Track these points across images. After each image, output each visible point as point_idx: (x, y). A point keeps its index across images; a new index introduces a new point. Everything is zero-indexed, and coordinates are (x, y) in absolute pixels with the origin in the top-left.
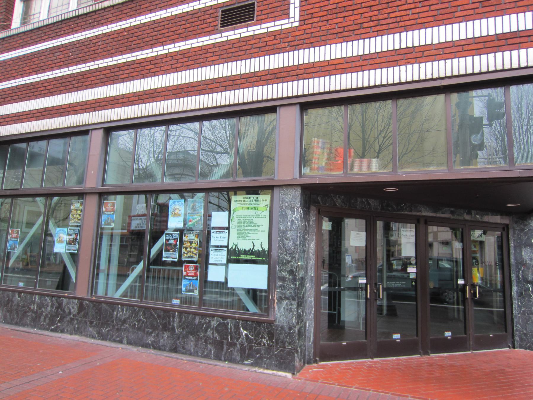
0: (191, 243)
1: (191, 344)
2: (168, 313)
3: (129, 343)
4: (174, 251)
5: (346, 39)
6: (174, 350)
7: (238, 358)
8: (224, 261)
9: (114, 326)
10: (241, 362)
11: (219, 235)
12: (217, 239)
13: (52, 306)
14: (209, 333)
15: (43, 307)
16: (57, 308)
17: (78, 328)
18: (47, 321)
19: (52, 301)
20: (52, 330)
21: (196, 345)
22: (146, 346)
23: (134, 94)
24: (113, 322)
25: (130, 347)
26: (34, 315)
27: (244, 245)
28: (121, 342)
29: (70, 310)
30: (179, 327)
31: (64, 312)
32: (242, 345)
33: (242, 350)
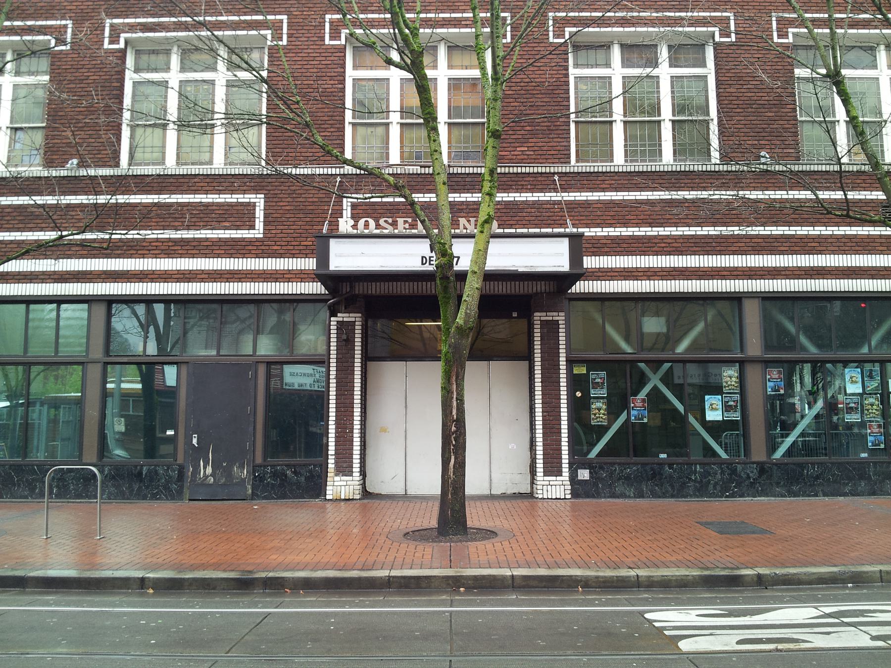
2: (863, 463)
3: (825, 495)
4: (857, 413)
9: (805, 483)
13: (723, 473)
15: (709, 474)
18: (718, 488)
19: (722, 469)
20: (727, 497)
22: (845, 495)
23: (800, 269)
24: (804, 479)
25: (827, 499)
29: (748, 475)
31: (740, 476)
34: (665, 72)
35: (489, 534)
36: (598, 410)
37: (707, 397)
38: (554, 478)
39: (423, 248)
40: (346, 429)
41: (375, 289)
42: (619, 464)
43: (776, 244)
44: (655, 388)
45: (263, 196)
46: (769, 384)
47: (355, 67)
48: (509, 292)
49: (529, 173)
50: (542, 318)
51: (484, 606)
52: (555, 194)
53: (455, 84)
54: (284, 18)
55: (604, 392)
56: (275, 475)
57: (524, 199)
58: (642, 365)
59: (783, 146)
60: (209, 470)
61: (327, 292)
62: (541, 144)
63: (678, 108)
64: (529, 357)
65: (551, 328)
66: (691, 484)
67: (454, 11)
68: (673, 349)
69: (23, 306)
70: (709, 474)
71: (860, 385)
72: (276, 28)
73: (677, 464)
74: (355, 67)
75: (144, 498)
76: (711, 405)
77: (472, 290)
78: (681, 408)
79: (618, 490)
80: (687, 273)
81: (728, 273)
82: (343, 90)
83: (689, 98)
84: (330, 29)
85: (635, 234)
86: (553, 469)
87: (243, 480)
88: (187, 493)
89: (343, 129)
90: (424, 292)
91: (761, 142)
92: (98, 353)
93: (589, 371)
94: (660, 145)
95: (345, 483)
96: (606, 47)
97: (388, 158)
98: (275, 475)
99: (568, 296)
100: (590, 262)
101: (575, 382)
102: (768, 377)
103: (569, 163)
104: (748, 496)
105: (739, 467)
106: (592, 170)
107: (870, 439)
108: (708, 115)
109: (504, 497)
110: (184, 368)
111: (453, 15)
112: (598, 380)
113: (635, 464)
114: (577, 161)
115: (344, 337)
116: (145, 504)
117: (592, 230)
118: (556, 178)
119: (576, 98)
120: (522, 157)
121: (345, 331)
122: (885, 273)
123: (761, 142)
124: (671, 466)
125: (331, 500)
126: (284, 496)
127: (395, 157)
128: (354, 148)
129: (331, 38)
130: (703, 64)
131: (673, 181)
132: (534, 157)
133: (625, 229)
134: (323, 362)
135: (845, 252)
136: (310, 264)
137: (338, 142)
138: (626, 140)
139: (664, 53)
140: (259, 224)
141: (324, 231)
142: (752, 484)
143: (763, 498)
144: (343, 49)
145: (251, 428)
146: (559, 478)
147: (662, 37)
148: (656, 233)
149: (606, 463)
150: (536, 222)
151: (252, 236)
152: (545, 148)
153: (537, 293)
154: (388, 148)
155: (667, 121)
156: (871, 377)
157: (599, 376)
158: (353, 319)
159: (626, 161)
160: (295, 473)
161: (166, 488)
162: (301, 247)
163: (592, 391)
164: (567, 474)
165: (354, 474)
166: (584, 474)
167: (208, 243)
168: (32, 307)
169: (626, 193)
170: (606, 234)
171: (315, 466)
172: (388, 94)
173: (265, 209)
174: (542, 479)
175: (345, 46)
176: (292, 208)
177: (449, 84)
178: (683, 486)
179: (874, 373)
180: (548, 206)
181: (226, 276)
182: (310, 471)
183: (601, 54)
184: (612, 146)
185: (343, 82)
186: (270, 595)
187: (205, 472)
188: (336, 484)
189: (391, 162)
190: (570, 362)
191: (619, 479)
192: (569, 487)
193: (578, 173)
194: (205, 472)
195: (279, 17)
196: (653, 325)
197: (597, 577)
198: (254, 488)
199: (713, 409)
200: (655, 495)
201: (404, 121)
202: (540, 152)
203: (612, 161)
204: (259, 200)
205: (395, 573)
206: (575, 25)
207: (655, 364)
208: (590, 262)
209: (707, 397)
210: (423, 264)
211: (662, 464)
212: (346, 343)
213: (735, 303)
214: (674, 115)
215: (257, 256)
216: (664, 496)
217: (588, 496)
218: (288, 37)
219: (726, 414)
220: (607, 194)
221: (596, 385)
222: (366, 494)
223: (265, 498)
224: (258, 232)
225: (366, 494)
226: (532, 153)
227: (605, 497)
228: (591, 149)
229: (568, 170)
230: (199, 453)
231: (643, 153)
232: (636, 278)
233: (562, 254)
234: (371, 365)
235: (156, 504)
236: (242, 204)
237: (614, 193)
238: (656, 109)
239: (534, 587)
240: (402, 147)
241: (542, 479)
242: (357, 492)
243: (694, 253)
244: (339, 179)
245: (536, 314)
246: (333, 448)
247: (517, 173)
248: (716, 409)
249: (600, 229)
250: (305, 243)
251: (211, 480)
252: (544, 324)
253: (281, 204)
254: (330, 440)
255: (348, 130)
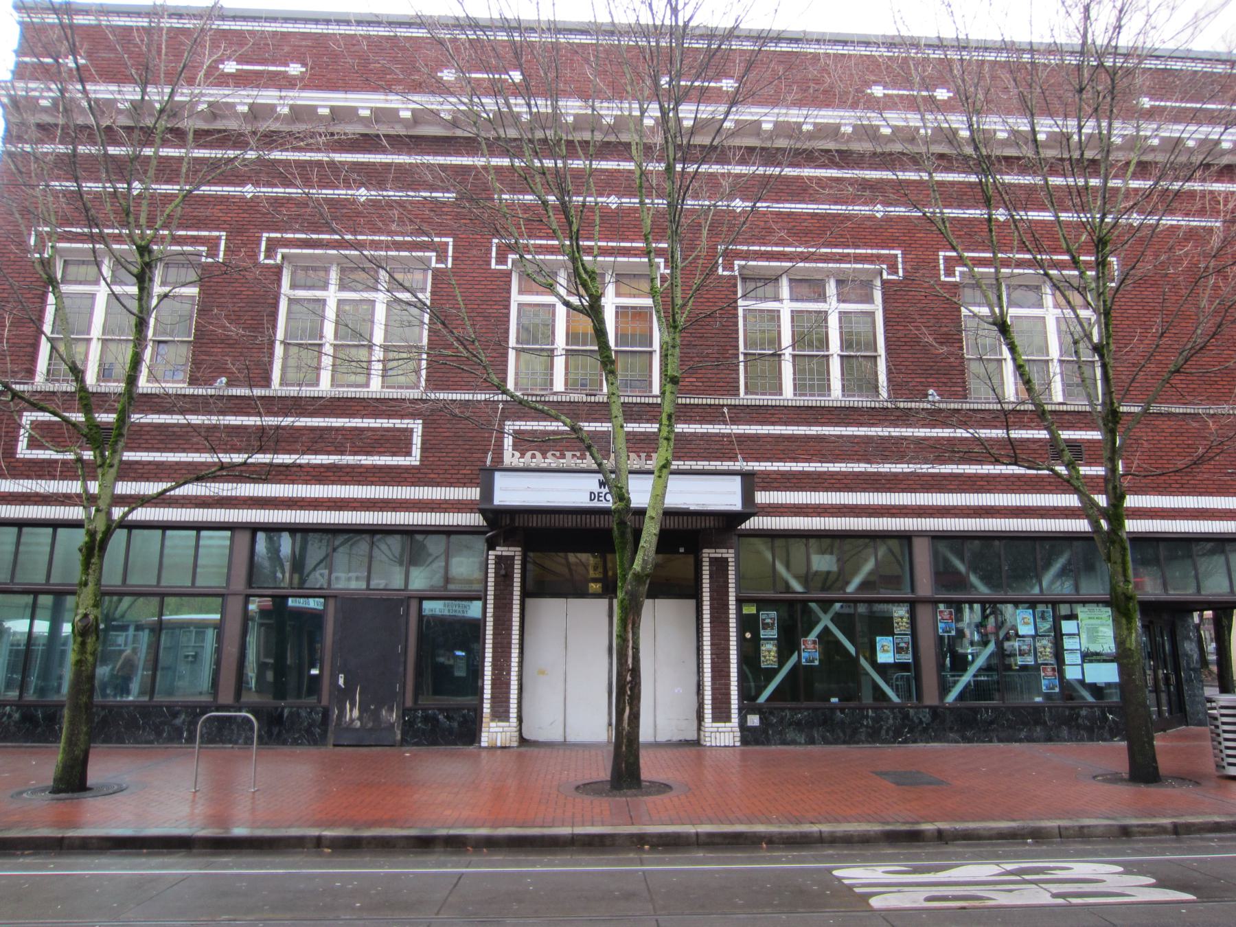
0: (1045, 648)
1: (1065, 732)
2: (1037, 709)
3: (1000, 740)
5: (1161, 493)
6: (1049, 739)
7: (1108, 737)
8: (1079, 661)
10: (1111, 739)
11: (1071, 640)
12: (1068, 643)
13: (895, 718)
14: (1080, 721)
15: (882, 720)
16: (903, 719)
17: (935, 736)
18: (891, 733)
19: (894, 713)
20: (900, 742)
21: (1070, 733)
22: (1020, 741)
25: (1002, 745)
26: (870, 730)
27: (1094, 648)
28: (990, 741)
30: (1050, 720)
31: (912, 721)
32: (1110, 727)
33: (1111, 730)
34: (833, 307)
35: (664, 788)
36: (769, 652)
37: (878, 638)
38: (723, 724)
39: (591, 483)
40: (503, 670)
41: (534, 522)
42: (790, 709)
43: (944, 482)
44: (826, 629)
45: (421, 421)
46: (940, 625)
47: (521, 292)
48: (676, 526)
49: (698, 405)
50: (712, 555)
51: (675, 865)
52: (724, 427)
53: (621, 311)
54: (450, 240)
55: (773, 633)
56: (426, 719)
57: (693, 431)
58: (813, 605)
59: (950, 384)
60: (356, 713)
61: (485, 524)
62: (710, 376)
63: (846, 343)
64: (696, 595)
65: (720, 566)
66: (863, 730)
67: (623, 240)
68: (843, 588)
69: (159, 532)
70: (881, 719)
71: (1032, 626)
72: (441, 251)
73: (849, 708)
74: (521, 292)
75: (284, 743)
76: (883, 646)
77: (650, 531)
78: (852, 649)
79: (790, 735)
80: (857, 511)
81: (898, 511)
82: (508, 315)
83: (858, 334)
84: (497, 254)
85: (805, 469)
86: (721, 714)
87: (392, 725)
88: (331, 741)
89: (505, 355)
90: (588, 525)
91: (930, 380)
92: (239, 584)
93: (758, 611)
94: (829, 380)
95: (501, 730)
96: (777, 279)
97: (552, 384)
98: (426, 719)
99: (737, 532)
100: (762, 497)
101: (747, 623)
102: (939, 618)
103: (739, 395)
104: (922, 741)
105: (912, 712)
106: (761, 404)
107: (1043, 682)
108: (876, 350)
109: (669, 745)
110: (331, 602)
111: (623, 244)
112: (768, 621)
113: (807, 709)
114: (746, 393)
115: (503, 572)
116: (286, 749)
117: (762, 464)
118: (725, 410)
119: (745, 331)
120: (690, 388)
121: (504, 564)
122: (1054, 512)
123: (930, 380)
124: (842, 711)
125: (485, 748)
126: (434, 743)
127: (559, 385)
128: (517, 374)
129: (497, 263)
130: (869, 299)
131: (842, 416)
132: (702, 388)
133: (795, 464)
134: (478, 599)
135: (1013, 491)
136: (473, 493)
137: (501, 367)
138: (794, 373)
139: (831, 288)
140: (416, 451)
141: (488, 463)
142: (925, 730)
143: (935, 744)
144: (508, 274)
145: (401, 669)
146: (728, 724)
147: (830, 273)
148: (826, 469)
149: (776, 709)
150: (705, 455)
151: (408, 463)
152: (714, 380)
153: (705, 529)
154: (552, 375)
155: (835, 356)
156: (1043, 618)
157: (769, 616)
158: (512, 554)
159: (795, 395)
160: (447, 717)
161: (309, 731)
162: (459, 476)
163: (762, 632)
164: (737, 720)
165: (511, 720)
166: (754, 720)
167: (362, 470)
168: (169, 533)
169: (796, 428)
170: (776, 469)
171: (469, 710)
172: (554, 321)
173: (423, 436)
174: (710, 725)
175: (511, 271)
176: (452, 434)
177: (617, 313)
178: (855, 732)
179: (1046, 615)
180: (718, 439)
181: (380, 505)
182: (464, 716)
183: (769, 289)
184: (780, 379)
185: (508, 307)
186: (452, 854)
187: (351, 715)
188: (491, 730)
189: (555, 389)
190: (740, 601)
191: (790, 724)
192: (739, 734)
193: (748, 406)
194: (351, 715)
195: (444, 239)
196: (823, 563)
197: (781, 833)
198: (403, 734)
199: (885, 651)
200: (827, 742)
201: (569, 348)
202: (709, 384)
203: (781, 394)
204: (417, 427)
205: (579, 830)
206: (744, 259)
207: (826, 604)
208: (762, 497)
209: (878, 638)
210: (591, 500)
211: (833, 709)
212: (504, 579)
213: (905, 542)
214: (842, 350)
215: (413, 484)
216: (836, 742)
217: (757, 742)
218: (453, 260)
219: (897, 656)
220: (777, 427)
221: (766, 626)
222: (523, 741)
223: (416, 744)
224: (414, 459)
225: (523, 741)
226: (700, 384)
227: (775, 744)
228: (760, 382)
229: (737, 403)
230: (345, 695)
231: (812, 387)
232: (806, 515)
233: (735, 493)
234: (530, 602)
235: (298, 750)
236: (399, 430)
237: (784, 428)
238: (824, 342)
239: (718, 844)
240: (566, 374)
241: (710, 725)
242: (514, 739)
243: (864, 490)
244: (501, 406)
245: (705, 551)
246: (489, 692)
247: (686, 405)
248: (887, 651)
249: (770, 464)
250: (465, 472)
251: (358, 724)
252: (713, 561)
253: (440, 430)
254: (486, 682)
255: (512, 355)
